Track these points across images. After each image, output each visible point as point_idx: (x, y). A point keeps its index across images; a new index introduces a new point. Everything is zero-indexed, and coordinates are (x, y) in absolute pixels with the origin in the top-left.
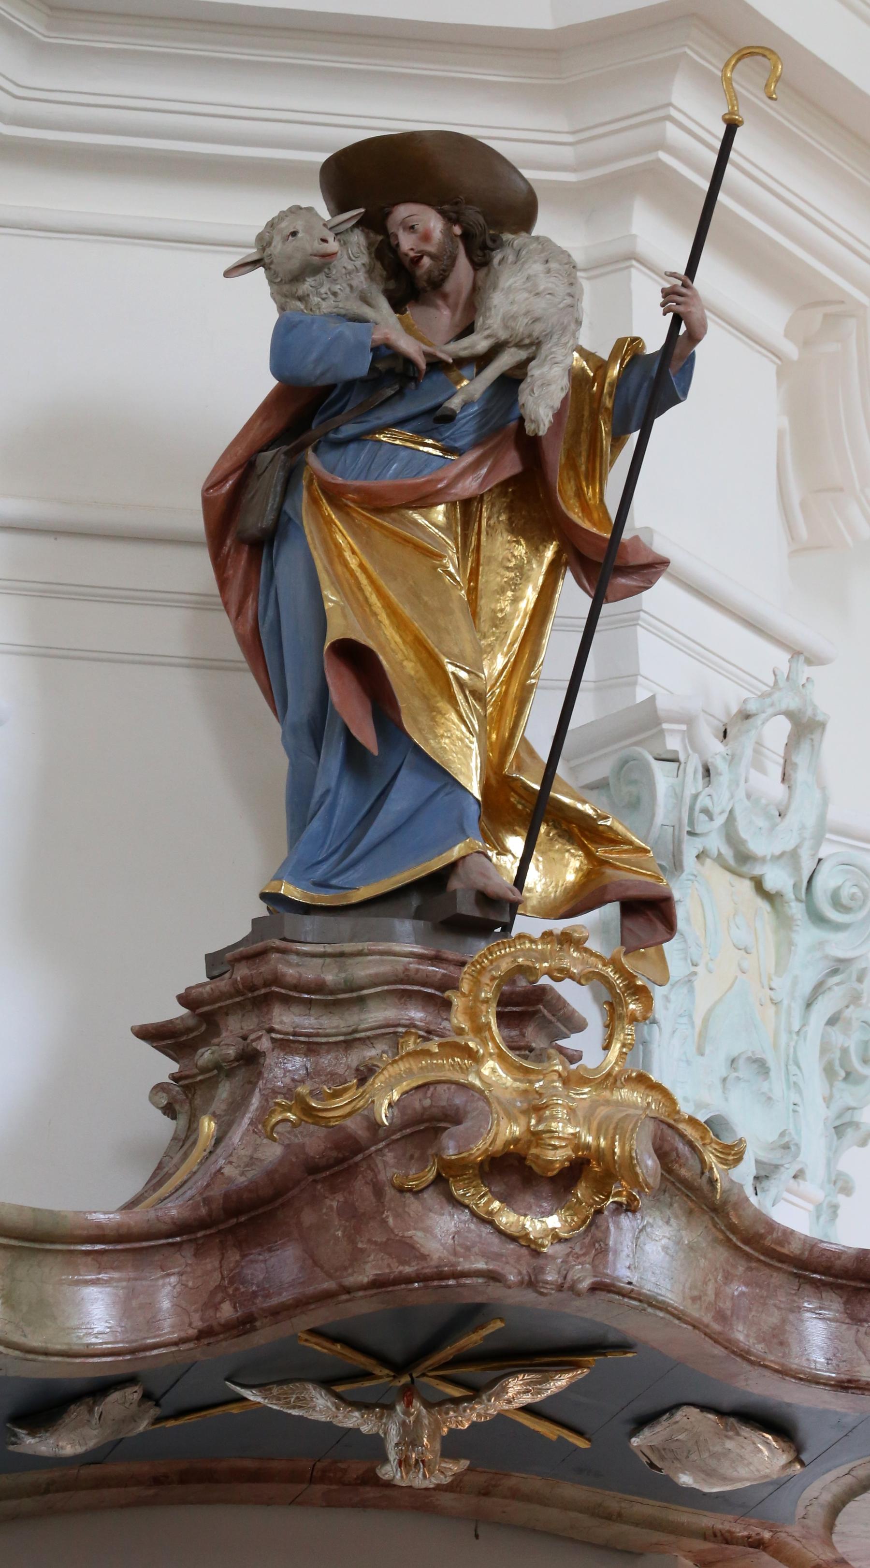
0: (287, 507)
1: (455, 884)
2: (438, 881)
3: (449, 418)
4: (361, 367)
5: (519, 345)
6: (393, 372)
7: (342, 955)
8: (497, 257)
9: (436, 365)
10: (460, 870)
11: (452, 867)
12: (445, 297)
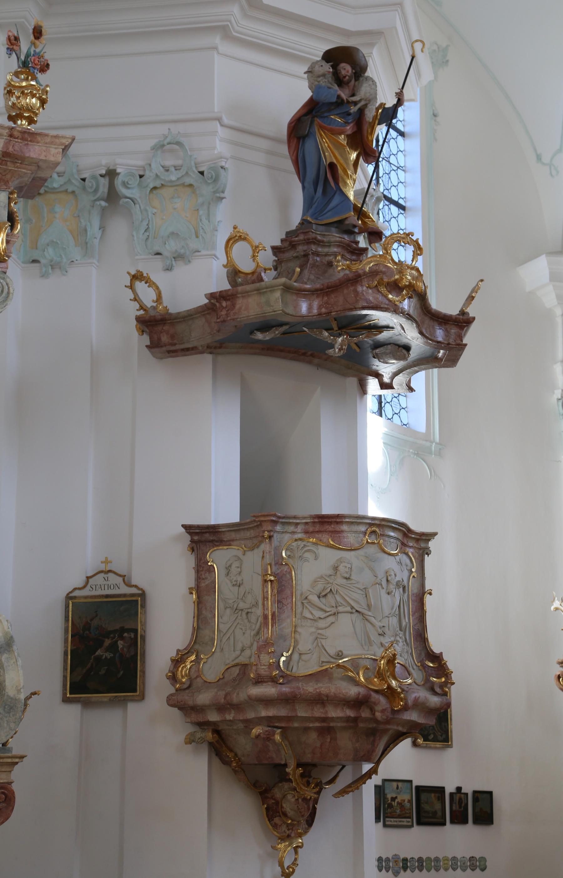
0: (311, 130)
1: (347, 222)
2: (341, 222)
3: (349, 114)
4: (334, 99)
5: (365, 100)
6: (340, 103)
7: (324, 235)
8: (361, 79)
9: (348, 102)
10: (349, 219)
11: (346, 218)
12: (348, 86)
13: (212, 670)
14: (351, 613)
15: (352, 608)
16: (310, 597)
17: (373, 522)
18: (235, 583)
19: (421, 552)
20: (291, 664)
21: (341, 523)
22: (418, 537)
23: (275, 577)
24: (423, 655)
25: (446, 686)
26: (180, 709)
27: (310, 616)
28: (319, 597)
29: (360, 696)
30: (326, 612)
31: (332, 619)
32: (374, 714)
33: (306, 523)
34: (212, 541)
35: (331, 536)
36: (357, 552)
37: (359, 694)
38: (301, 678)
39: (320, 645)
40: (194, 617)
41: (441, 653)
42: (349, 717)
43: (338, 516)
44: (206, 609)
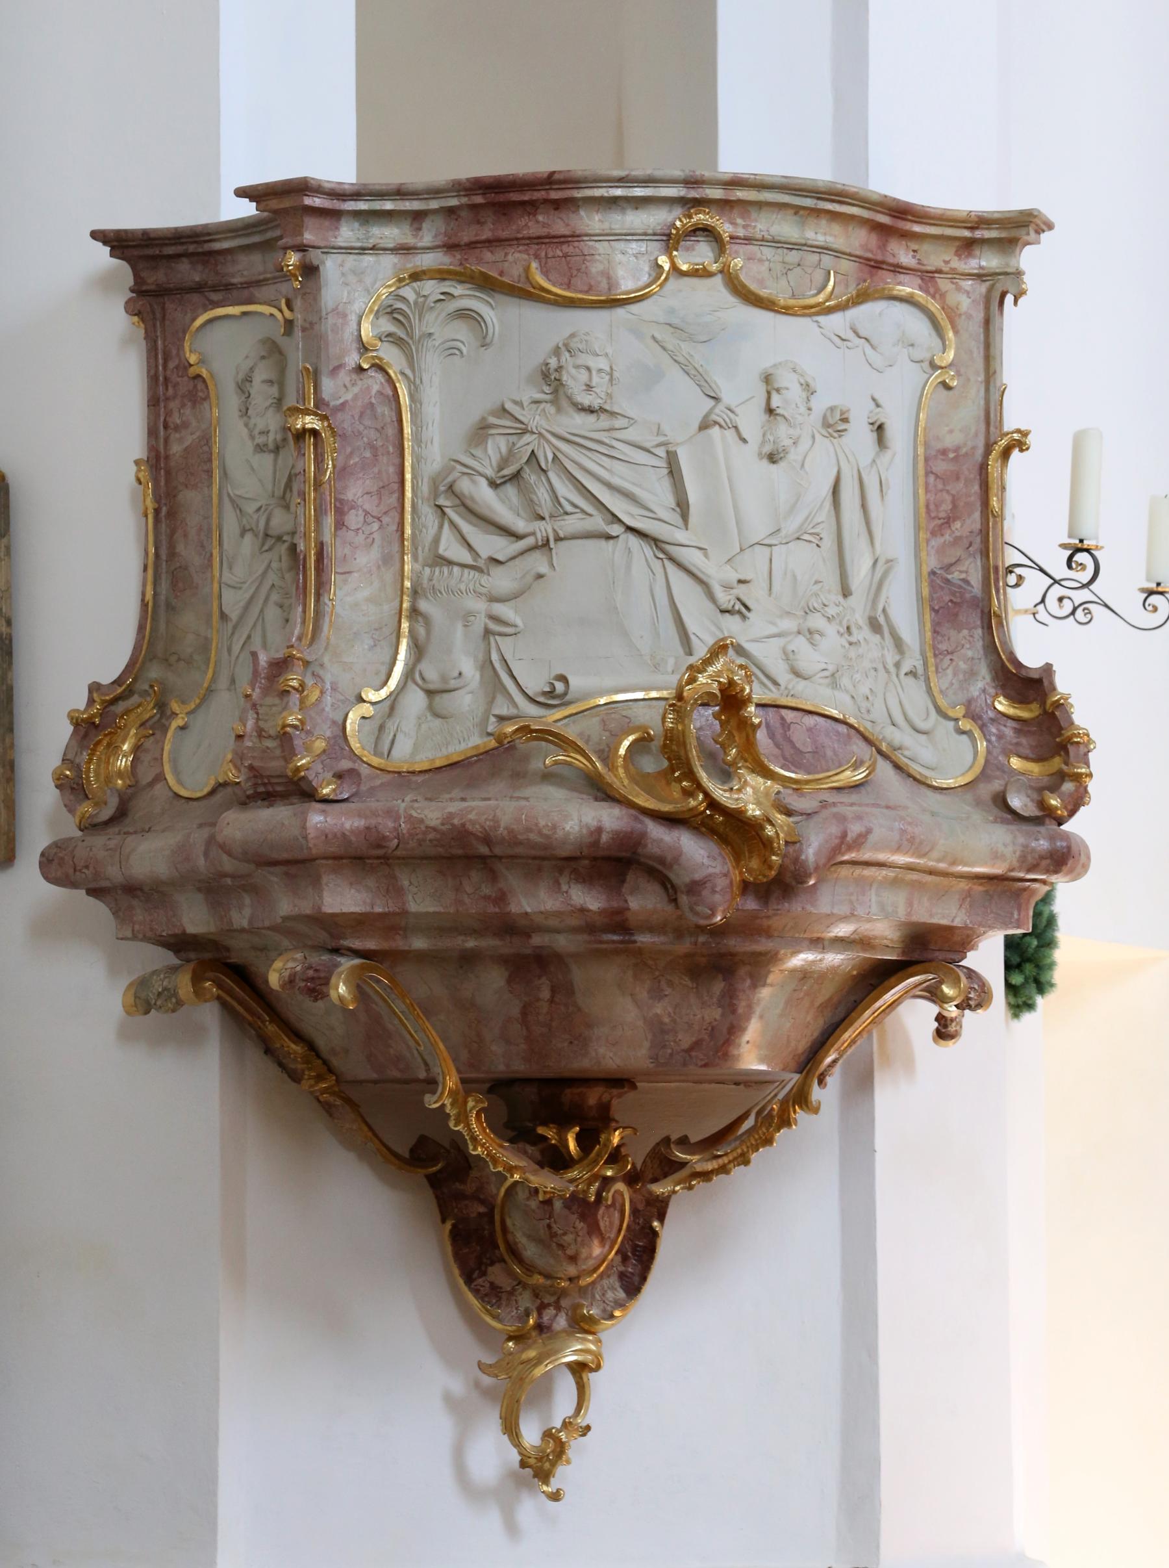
13: (201, 751)
14: (609, 537)
15: (616, 519)
16: (464, 486)
17: (693, 194)
18: (260, 440)
19: (983, 288)
20: (391, 727)
21: (571, 204)
22: (967, 234)
23: (324, 418)
24: (983, 680)
25: (1054, 789)
26: (93, 892)
27: (459, 553)
28: (493, 484)
29: (604, 838)
30: (518, 537)
31: (538, 563)
32: (674, 901)
33: (450, 211)
34: (198, 288)
35: (537, 256)
36: (634, 308)
37: (599, 830)
38: (420, 779)
39: (495, 657)
40: (145, 569)
41: (1048, 669)
42: (583, 910)
43: (550, 181)
44: (185, 536)
